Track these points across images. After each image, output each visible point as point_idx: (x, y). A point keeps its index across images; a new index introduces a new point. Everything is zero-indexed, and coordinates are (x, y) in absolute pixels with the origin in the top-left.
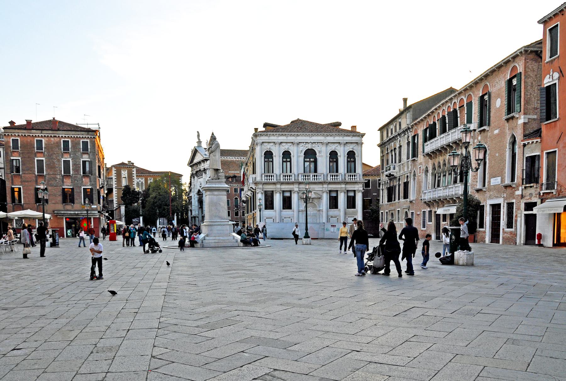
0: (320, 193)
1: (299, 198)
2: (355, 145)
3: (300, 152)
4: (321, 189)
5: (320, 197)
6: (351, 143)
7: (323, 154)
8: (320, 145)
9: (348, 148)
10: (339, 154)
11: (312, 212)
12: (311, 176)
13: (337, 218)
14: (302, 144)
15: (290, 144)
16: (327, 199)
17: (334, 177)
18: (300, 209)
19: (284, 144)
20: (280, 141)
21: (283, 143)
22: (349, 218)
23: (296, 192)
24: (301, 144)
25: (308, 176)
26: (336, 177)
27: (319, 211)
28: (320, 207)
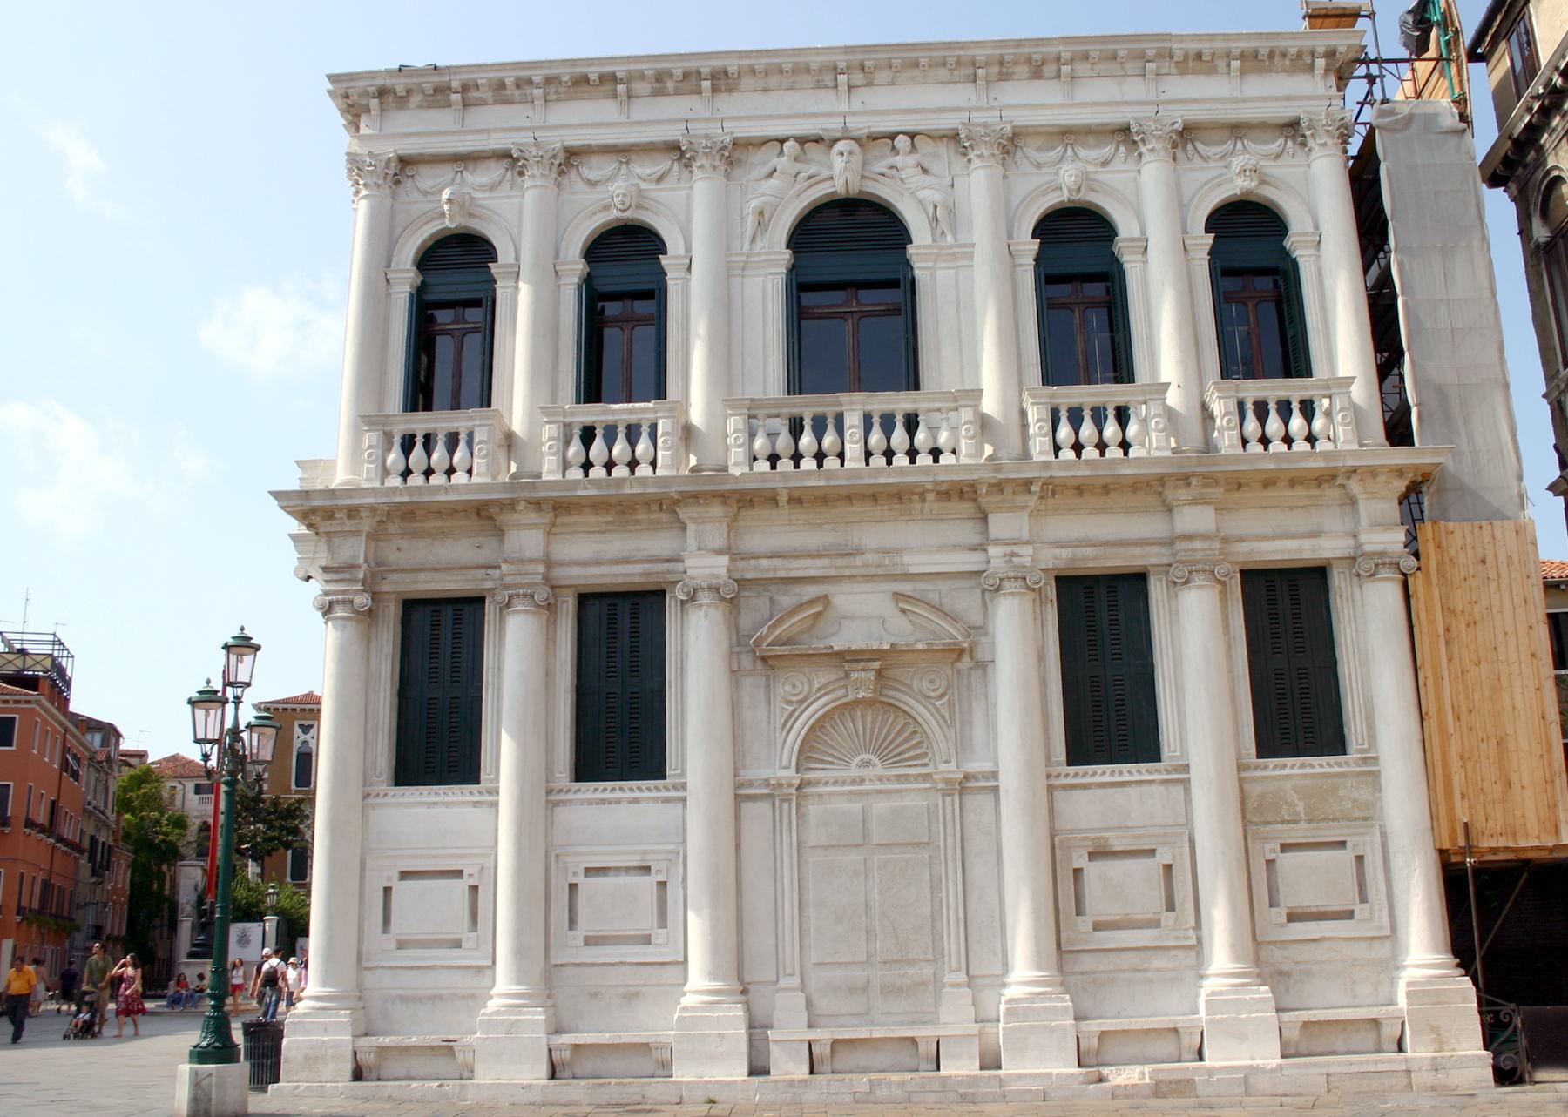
0: (966, 602)
1: (747, 662)
2: (1274, 147)
3: (750, 222)
4: (970, 561)
5: (955, 633)
6: (1237, 130)
7: (981, 230)
8: (941, 157)
9: (1213, 170)
10: (1126, 227)
11: (880, 806)
12: (853, 421)
13: (1164, 856)
14: (767, 158)
15: (663, 163)
16: (1042, 658)
17: (1087, 430)
18: (747, 775)
19: (596, 168)
20: (556, 141)
21: (595, 160)
22: (1287, 861)
23: (704, 599)
24: (757, 156)
25: (819, 433)
26: (1111, 430)
27: (963, 786)
28: (963, 746)
